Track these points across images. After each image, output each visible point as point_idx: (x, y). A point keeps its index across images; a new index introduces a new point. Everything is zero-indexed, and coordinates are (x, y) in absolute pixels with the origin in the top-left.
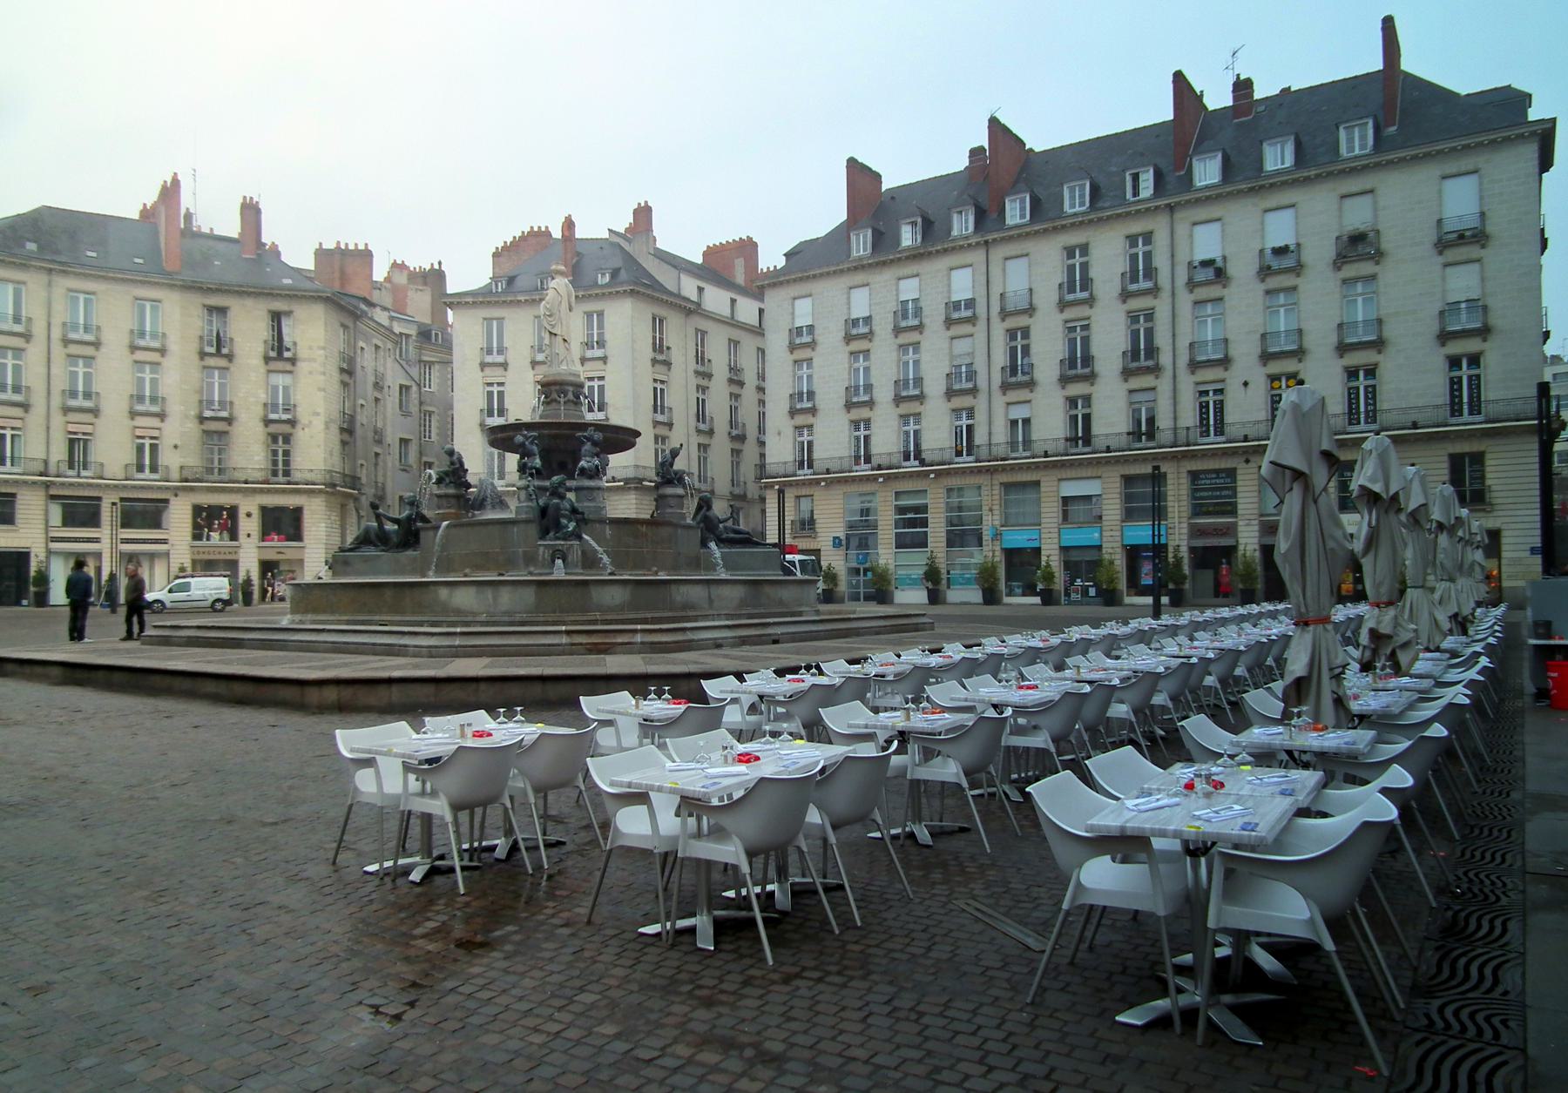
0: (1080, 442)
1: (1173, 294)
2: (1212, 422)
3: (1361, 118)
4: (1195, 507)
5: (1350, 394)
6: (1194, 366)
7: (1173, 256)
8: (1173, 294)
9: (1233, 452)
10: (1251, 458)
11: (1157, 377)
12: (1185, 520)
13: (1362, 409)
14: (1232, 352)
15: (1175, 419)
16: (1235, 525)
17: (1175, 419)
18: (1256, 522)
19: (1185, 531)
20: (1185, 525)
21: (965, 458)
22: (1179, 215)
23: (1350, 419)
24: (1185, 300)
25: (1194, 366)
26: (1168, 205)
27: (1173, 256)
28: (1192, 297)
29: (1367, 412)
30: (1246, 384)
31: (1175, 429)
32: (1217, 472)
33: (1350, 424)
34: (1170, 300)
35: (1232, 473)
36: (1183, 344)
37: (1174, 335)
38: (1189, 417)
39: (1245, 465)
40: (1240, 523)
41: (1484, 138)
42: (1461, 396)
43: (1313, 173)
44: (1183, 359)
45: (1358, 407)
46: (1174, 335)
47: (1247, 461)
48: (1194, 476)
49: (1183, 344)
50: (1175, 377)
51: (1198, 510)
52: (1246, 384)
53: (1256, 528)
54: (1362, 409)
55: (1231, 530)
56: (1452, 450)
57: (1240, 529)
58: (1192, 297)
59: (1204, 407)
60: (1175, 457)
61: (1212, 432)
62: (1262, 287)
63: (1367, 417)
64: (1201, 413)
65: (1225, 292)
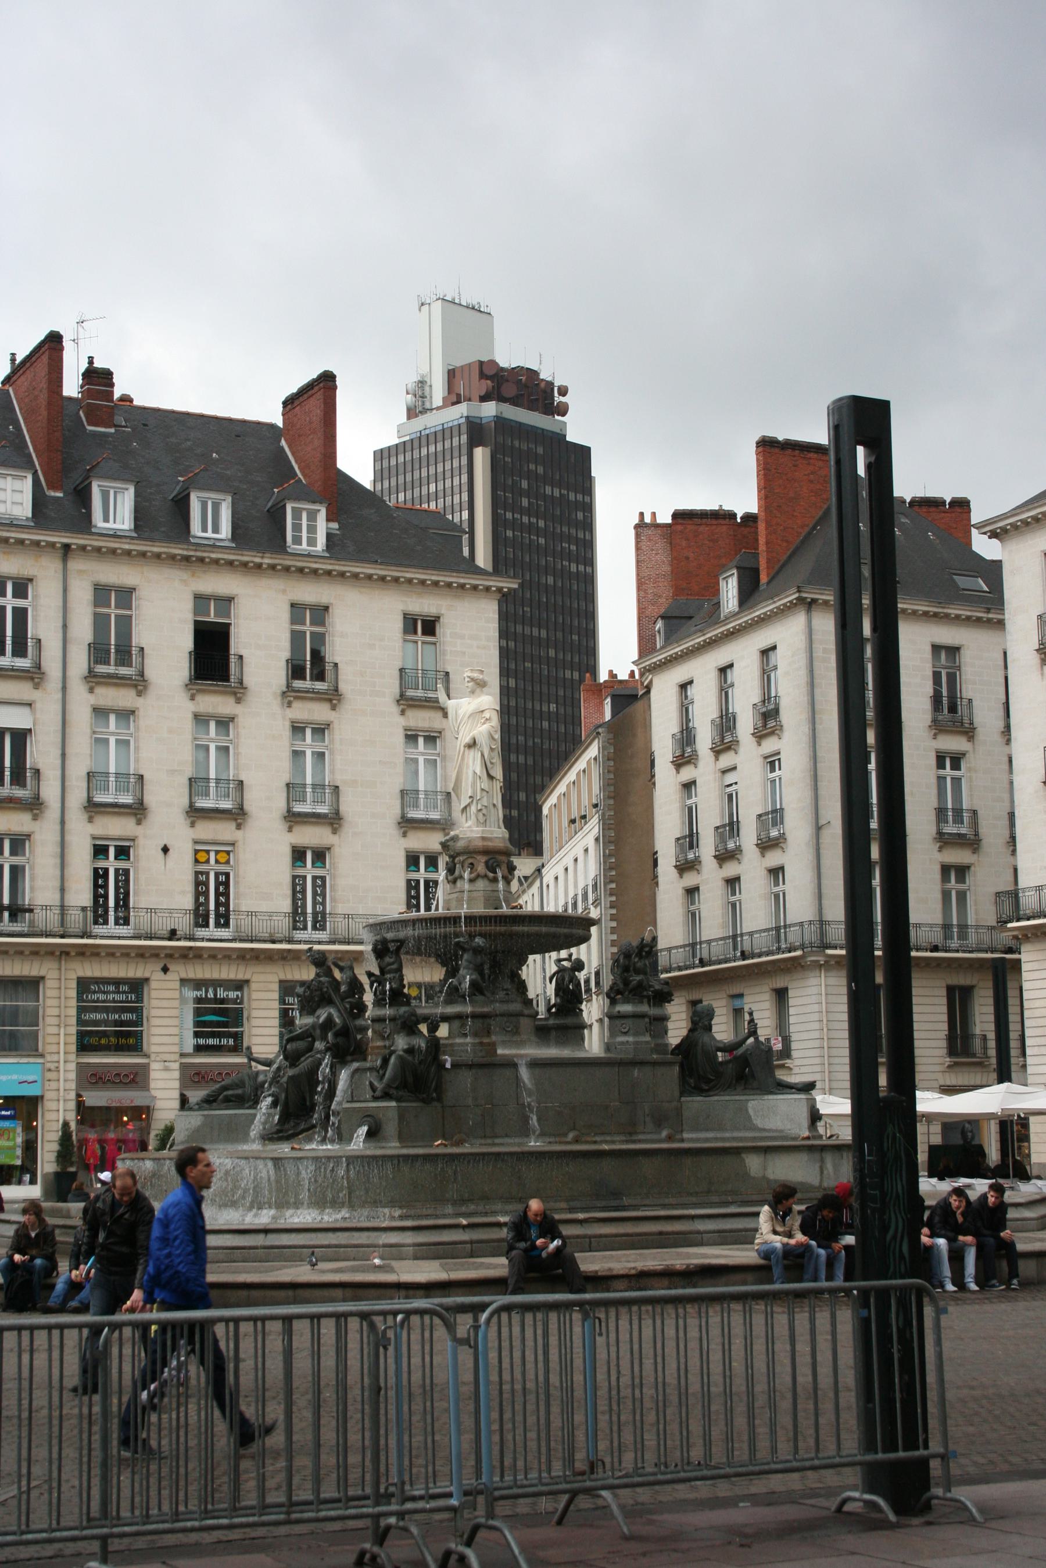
0: (6, 914)
1: (64, 688)
2: (111, 903)
3: (314, 502)
4: (81, 1035)
5: (294, 885)
6: (93, 808)
7: (65, 626)
8: (64, 688)
9: (142, 954)
10: (171, 967)
11: (35, 818)
12: (73, 1057)
13: (309, 910)
14: (149, 799)
15: (62, 890)
16: (146, 1068)
17: (62, 890)
18: (176, 1066)
19: (73, 1076)
20: (72, 1066)
21: (111, 928)
22: (75, 565)
23: (295, 921)
24: (82, 701)
25: (93, 808)
26: (67, 547)
27: (65, 626)
28: (92, 700)
29: (315, 914)
30: (165, 850)
31: (63, 907)
32: (117, 982)
33: (295, 928)
34: (60, 695)
35: (137, 986)
36: (78, 769)
37: (63, 755)
38: (81, 895)
39: (160, 975)
40: (154, 1066)
41: (443, 578)
42: (106, 897)
43: (267, 561)
44: (77, 795)
45: (304, 905)
46: (63, 755)
47: (165, 970)
48: (84, 985)
49: (78, 769)
50: (63, 822)
51: (85, 1044)
52: (165, 850)
53: (176, 1074)
54: (309, 910)
55: (137, 1078)
56: (81, 974)
57: (153, 1075)
58: (92, 700)
59: (99, 876)
60: (64, 954)
61: (212, 921)
62: (190, 707)
63: (218, 916)
64: (96, 886)
65: (139, 703)
